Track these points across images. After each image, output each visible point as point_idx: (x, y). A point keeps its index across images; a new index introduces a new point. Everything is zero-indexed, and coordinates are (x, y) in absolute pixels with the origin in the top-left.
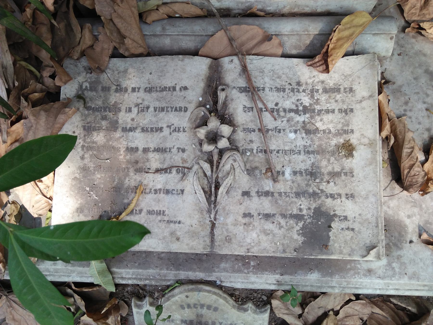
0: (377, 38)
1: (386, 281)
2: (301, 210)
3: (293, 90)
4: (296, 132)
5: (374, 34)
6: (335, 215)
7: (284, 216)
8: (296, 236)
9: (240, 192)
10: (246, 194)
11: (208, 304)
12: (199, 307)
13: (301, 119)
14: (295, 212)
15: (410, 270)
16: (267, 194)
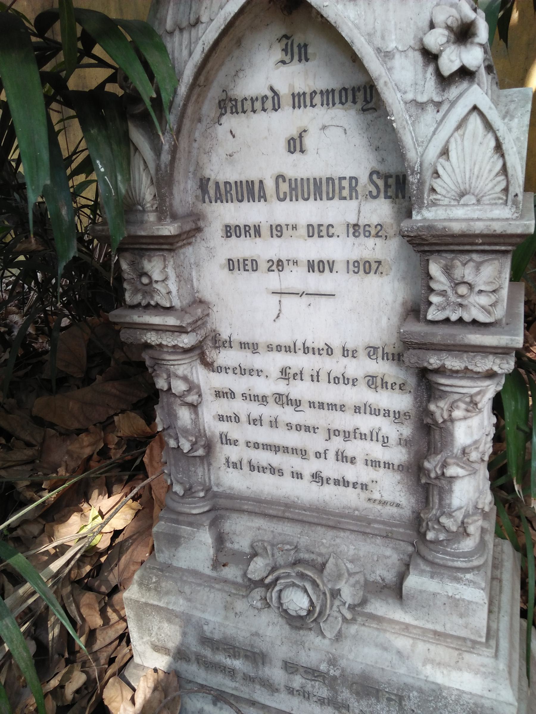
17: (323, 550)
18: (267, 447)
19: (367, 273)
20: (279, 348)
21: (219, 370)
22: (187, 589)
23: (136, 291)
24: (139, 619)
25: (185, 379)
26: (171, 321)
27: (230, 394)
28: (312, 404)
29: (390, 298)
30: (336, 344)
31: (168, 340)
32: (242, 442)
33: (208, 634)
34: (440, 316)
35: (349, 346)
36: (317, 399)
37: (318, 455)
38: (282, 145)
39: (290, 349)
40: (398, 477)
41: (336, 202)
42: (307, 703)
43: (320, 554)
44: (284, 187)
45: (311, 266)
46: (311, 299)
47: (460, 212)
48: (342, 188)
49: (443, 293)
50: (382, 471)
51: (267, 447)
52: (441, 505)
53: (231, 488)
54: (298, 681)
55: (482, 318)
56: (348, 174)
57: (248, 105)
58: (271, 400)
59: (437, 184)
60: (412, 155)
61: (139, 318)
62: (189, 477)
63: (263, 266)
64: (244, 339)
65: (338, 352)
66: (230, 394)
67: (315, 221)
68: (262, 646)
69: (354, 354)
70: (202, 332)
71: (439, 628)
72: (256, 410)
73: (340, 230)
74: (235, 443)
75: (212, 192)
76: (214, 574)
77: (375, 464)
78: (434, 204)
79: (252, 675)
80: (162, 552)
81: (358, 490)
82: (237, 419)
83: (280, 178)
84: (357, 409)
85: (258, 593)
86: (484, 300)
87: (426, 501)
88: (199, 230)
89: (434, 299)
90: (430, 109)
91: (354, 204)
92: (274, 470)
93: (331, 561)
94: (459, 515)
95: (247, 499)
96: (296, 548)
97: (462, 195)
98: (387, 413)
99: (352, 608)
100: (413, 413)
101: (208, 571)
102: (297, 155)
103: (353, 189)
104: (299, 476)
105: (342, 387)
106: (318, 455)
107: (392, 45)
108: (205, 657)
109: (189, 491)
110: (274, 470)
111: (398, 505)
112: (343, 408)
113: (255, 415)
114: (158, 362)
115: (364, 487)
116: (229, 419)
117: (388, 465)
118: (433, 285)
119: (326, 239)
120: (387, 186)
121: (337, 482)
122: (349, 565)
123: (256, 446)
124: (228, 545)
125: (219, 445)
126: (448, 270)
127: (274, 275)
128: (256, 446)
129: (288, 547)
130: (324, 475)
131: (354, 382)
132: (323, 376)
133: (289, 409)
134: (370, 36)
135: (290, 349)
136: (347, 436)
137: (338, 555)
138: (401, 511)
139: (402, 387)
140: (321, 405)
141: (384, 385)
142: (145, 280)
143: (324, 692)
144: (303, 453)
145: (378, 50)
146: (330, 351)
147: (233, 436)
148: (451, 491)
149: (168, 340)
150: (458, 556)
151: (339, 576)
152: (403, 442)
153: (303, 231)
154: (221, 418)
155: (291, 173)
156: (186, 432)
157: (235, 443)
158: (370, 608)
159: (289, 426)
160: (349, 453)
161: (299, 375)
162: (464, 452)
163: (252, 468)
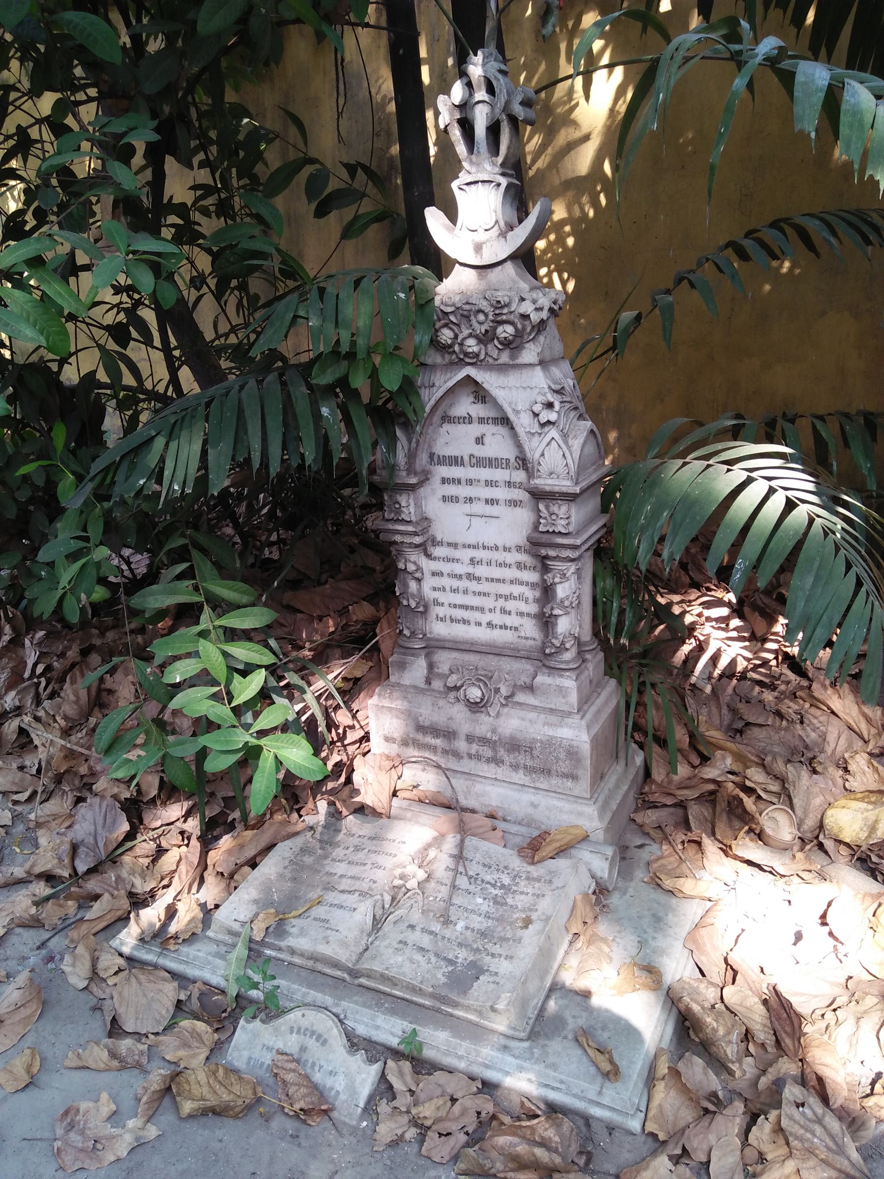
0: (593, 856)
2: (457, 957)
3: (498, 870)
4: (485, 899)
6: (487, 970)
7: (437, 955)
8: (439, 976)
11: (320, 1031)
15: (551, 1059)
18: (462, 607)
20: (469, 546)
21: (434, 559)
22: (410, 696)
25: (415, 563)
26: (410, 528)
27: (439, 574)
28: (487, 579)
29: (527, 520)
30: (500, 545)
31: (407, 540)
32: (446, 604)
34: (545, 529)
35: (507, 546)
36: (490, 576)
37: (490, 611)
38: (473, 440)
39: (475, 547)
41: (499, 470)
44: (474, 461)
45: (487, 501)
49: (545, 518)
51: (462, 607)
54: (474, 748)
55: (563, 531)
59: (540, 468)
60: (528, 455)
63: (462, 500)
65: (501, 549)
66: (439, 574)
67: (489, 479)
68: (454, 726)
69: (510, 550)
70: (426, 536)
71: (553, 707)
72: (455, 583)
73: (501, 484)
77: (522, 614)
78: (540, 477)
82: (444, 589)
83: (471, 456)
84: (512, 582)
85: (452, 695)
86: (563, 522)
87: (546, 636)
88: (428, 479)
89: (542, 521)
91: (508, 471)
92: (465, 622)
94: (561, 637)
95: (449, 641)
96: (477, 669)
98: (527, 584)
99: (506, 698)
101: (423, 685)
102: (480, 446)
103: (507, 464)
106: (490, 611)
109: (413, 633)
110: (465, 622)
114: (400, 553)
115: (516, 629)
116: (439, 589)
117: (528, 615)
121: (501, 627)
123: (455, 606)
124: (436, 670)
126: (547, 507)
128: (455, 606)
132: (493, 563)
133: (474, 582)
134: (510, 404)
135: (475, 547)
136: (507, 598)
137: (500, 670)
139: (534, 568)
140: (492, 580)
141: (525, 567)
142: (397, 506)
143: (488, 753)
144: (482, 610)
147: (441, 600)
149: (407, 540)
150: (562, 662)
151: (500, 681)
152: (536, 601)
153: (483, 483)
154: (434, 589)
155: (477, 454)
156: (413, 596)
160: (508, 609)
161: (480, 562)
162: (562, 602)
163: (452, 620)
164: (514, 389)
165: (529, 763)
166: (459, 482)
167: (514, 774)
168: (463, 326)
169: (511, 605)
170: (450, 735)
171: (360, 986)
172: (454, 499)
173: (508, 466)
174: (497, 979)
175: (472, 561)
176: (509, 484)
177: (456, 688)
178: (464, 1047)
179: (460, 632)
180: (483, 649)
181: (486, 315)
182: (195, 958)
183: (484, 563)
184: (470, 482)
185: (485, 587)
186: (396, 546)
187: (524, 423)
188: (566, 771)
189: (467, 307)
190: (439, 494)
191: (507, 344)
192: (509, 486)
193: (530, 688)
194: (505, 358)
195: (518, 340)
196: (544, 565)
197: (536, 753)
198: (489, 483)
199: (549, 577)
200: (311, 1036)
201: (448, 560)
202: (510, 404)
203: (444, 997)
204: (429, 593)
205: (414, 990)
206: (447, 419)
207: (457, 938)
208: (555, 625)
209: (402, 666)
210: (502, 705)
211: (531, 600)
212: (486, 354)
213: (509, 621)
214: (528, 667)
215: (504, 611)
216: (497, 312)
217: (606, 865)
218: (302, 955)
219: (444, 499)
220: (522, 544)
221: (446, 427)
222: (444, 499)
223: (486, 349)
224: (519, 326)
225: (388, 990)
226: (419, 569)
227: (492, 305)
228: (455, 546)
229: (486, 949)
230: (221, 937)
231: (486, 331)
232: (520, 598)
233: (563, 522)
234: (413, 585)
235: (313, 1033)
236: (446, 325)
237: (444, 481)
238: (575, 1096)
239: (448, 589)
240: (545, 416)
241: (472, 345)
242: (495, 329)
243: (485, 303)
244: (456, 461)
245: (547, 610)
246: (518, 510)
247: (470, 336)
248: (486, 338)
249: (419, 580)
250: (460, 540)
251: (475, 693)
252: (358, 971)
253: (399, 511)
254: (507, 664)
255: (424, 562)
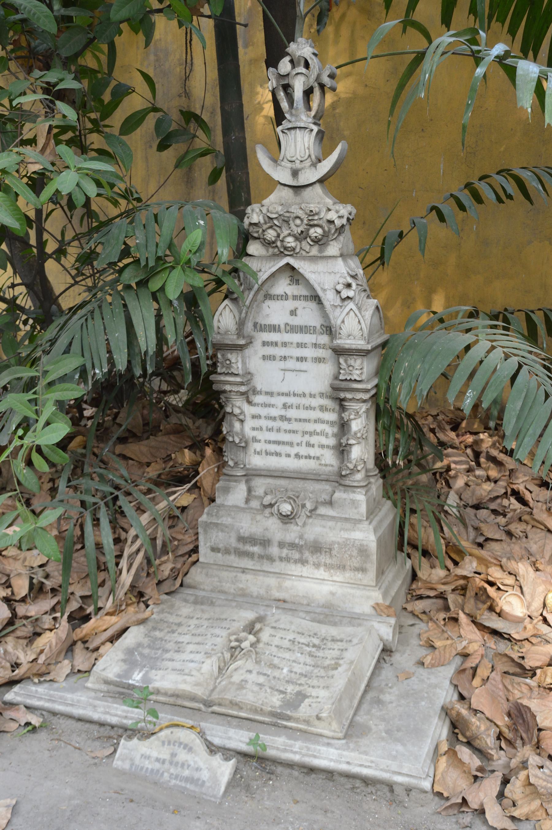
0: (381, 625)
1: (340, 751)
3: (310, 636)
4: (302, 654)
5: (379, 622)
7: (271, 688)
9: (245, 670)
10: (250, 672)
12: (177, 744)
13: (308, 649)
14: (281, 689)
16: (265, 675)
17: (299, 490)
19: (320, 362)
20: (283, 394)
22: (233, 514)
23: (223, 367)
24: (205, 531)
25: (239, 408)
26: (238, 379)
28: (296, 420)
29: (328, 373)
30: (307, 392)
31: (235, 389)
33: (242, 535)
34: (344, 378)
35: (312, 393)
36: (298, 417)
37: (298, 444)
38: (288, 312)
39: (287, 395)
40: (332, 452)
41: (308, 335)
42: (288, 564)
43: (297, 492)
44: (288, 328)
45: (298, 359)
46: (297, 373)
47: (348, 341)
48: (310, 330)
49: (344, 369)
50: (325, 449)
52: (348, 459)
53: (256, 465)
54: (285, 552)
55: (358, 379)
56: (313, 325)
57: (276, 297)
58: (278, 419)
59: (341, 332)
60: (332, 322)
61: (222, 378)
62: (237, 457)
63: (278, 358)
64: (268, 390)
65: (308, 396)
67: (300, 341)
68: (268, 535)
70: (249, 386)
71: (347, 516)
72: (271, 424)
73: (309, 345)
74: (259, 441)
75: (258, 327)
76: (246, 506)
77: (322, 446)
78: (340, 338)
79: (263, 554)
80: (219, 497)
81: (315, 460)
82: (261, 429)
83: (287, 324)
84: (315, 421)
85: (267, 511)
86: (358, 372)
87: (342, 461)
88: (251, 342)
89: (342, 371)
90: (339, 307)
91: (315, 336)
92: (278, 454)
93: (302, 494)
94: (354, 462)
95: (264, 470)
96: (286, 490)
97: (349, 336)
98: (328, 422)
99: (311, 511)
100: (338, 421)
101: (243, 505)
102: (293, 317)
103: (314, 330)
104: (288, 456)
105: (309, 411)
106: (298, 444)
107: (326, 287)
108: (239, 549)
111: (332, 466)
112: (309, 421)
113: (270, 427)
115: (318, 458)
117: (328, 447)
118: (341, 367)
119: (304, 349)
120: (327, 330)
121: (306, 457)
122: (310, 495)
123: (270, 442)
124: (253, 493)
125: (251, 443)
126: (346, 361)
127: (282, 363)
128: (270, 442)
129: (282, 489)
130: (300, 454)
131: (314, 409)
132: (301, 407)
133: (286, 423)
134: (319, 284)
135: (287, 395)
136: (311, 434)
138: (334, 468)
140: (300, 420)
141: (326, 409)
142: (228, 362)
143: (297, 556)
144: (291, 444)
145: (322, 288)
146: (304, 395)
147: (259, 438)
148: (351, 452)
149: (235, 389)
150: (354, 481)
151: (306, 499)
152: (335, 435)
153: (295, 345)
154: (254, 429)
155: (291, 323)
156: (237, 434)
157: (259, 441)
158: (319, 511)
159: (285, 431)
160: (312, 443)
161: (291, 407)
163: (267, 453)
164: (322, 274)
165: (328, 561)
166: (276, 344)
167: (316, 571)
168: (283, 229)
169: (314, 440)
170: (265, 543)
171: (213, 713)
172: (272, 358)
173: (315, 332)
174: (319, 700)
175: (285, 406)
176: (315, 345)
177: (271, 505)
178: (298, 745)
179: (273, 462)
180: (292, 475)
181: (302, 220)
182: (78, 701)
183: (294, 407)
184: (285, 344)
185: (294, 426)
186: (225, 395)
187: (329, 298)
188: (357, 565)
189: (287, 215)
190: (260, 354)
191: (316, 241)
192: (315, 347)
193: (330, 503)
194: (314, 251)
195: (325, 239)
196: (341, 403)
197: (334, 552)
198: (300, 345)
199: (345, 415)
200: (179, 746)
201: (266, 405)
202: (319, 284)
203: (280, 714)
204: (249, 433)
205: (256, 711)
206: (268, 297)
207: (284, 677)
208: (349, 452)
209: (226, 490)
210: (308, 517)
211: (330, 435)
212: (301, 248)
213: (312, 452)
214: (327, 487)
215: (309, 445)
216: (310, 218)
217: (390, 631)
218: (165, 694)
219: (264, 358)
220: (324, 391)
221: (268, 303)
222: (264, 358)
223: (301, 245)
224: (326, 229)
225: (235, 713)
226: (242, 413)
227: (306, 214)
228: (270, 394)
229: (307, 684)
230: (97, 686)
231: (302, 232)
232: (322, 433)
233: (358, 372)
234: (237, 425)
235: (181, 744)
236: (271, 227)
237: (265, 344)
238: (381, 770)
239: (264, 428)
240: (345, 293)
241: (290, 242)
242: (308, 230)
243: (301, 212)
244: (274, 328)
245: (344, 441)
246: (322, 366)
247: (289, 235)
248: (301, 237)
249: (242, 421)
250: (275, 389)
251: (286, 508)
252: (211, 701)
253: (229, 366)
254: (311, 486)
255: (246, 407)
